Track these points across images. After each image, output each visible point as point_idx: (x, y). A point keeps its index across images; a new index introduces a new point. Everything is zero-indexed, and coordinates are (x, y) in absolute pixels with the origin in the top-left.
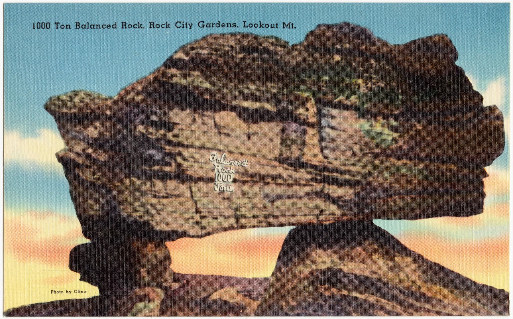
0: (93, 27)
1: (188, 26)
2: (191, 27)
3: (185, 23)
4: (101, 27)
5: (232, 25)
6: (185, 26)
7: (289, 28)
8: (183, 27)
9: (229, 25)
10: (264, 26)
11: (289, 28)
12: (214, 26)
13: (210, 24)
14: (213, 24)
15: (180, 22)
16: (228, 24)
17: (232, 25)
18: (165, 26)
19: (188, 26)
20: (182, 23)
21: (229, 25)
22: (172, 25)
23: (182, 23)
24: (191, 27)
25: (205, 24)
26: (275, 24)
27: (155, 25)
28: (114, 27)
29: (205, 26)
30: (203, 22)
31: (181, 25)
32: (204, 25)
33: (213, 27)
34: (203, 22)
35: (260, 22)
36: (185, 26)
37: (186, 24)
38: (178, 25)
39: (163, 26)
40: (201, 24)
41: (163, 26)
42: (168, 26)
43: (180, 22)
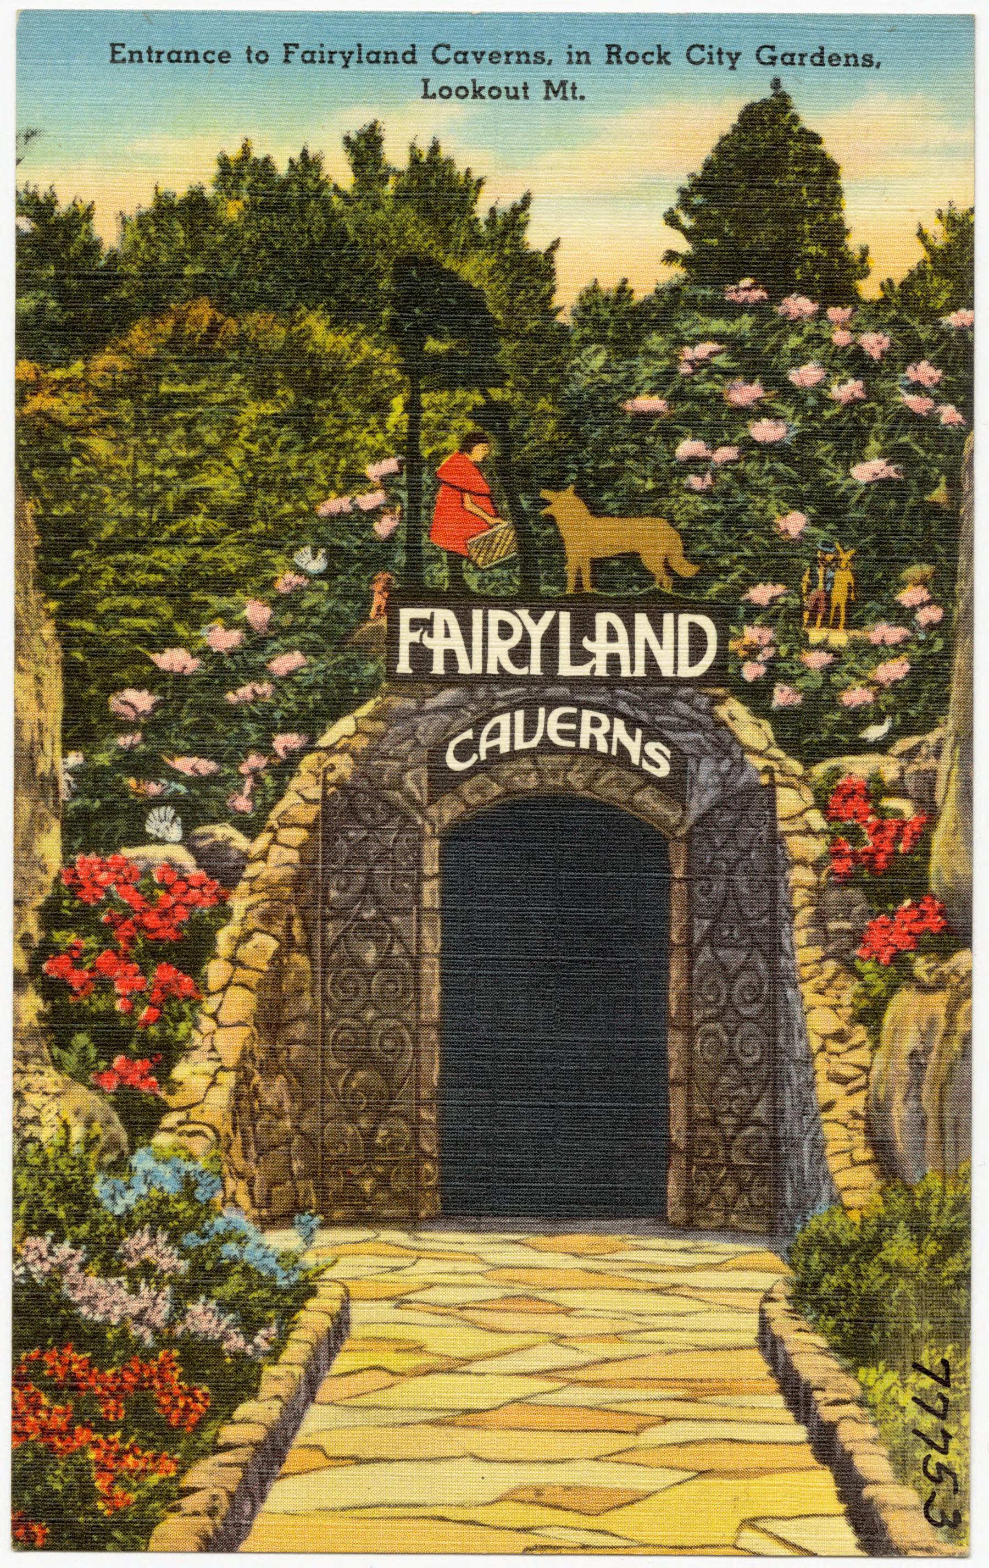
0: (192, 57)
1: (725, 58)
2: (734, 61)
3: (715, 50)
4: (201, 58)
5: (860, 61)
6: (716, 60)
7: (565, 98)
8: (711, 63)
9: (852, 61)
10: (485, 93)
11: (565, 98)
12: (807, 60)
15: (702, 47)
16: (847, 57)
17: (860, 61)
18: (655, 58)
19: (725, 58)
20: (707, 50)
21: (852, 61)
22: (679, 59)
23: (707, 50)
24: (734, 61)
25: (778, 53)
26: (520, 86)
28: (409, 57)
29: (779, 61)
30: (772, 48)
31: (704, 54)
32: (774, 58)
33: (802, 64)
34: (772, 48)
35: (474, 81)
36: (716, 60)
38: (696, 54)
39: (648, 58)
40: (765, 54)
41: (648, 58)
42: (663, 58)
43: (702, 47)
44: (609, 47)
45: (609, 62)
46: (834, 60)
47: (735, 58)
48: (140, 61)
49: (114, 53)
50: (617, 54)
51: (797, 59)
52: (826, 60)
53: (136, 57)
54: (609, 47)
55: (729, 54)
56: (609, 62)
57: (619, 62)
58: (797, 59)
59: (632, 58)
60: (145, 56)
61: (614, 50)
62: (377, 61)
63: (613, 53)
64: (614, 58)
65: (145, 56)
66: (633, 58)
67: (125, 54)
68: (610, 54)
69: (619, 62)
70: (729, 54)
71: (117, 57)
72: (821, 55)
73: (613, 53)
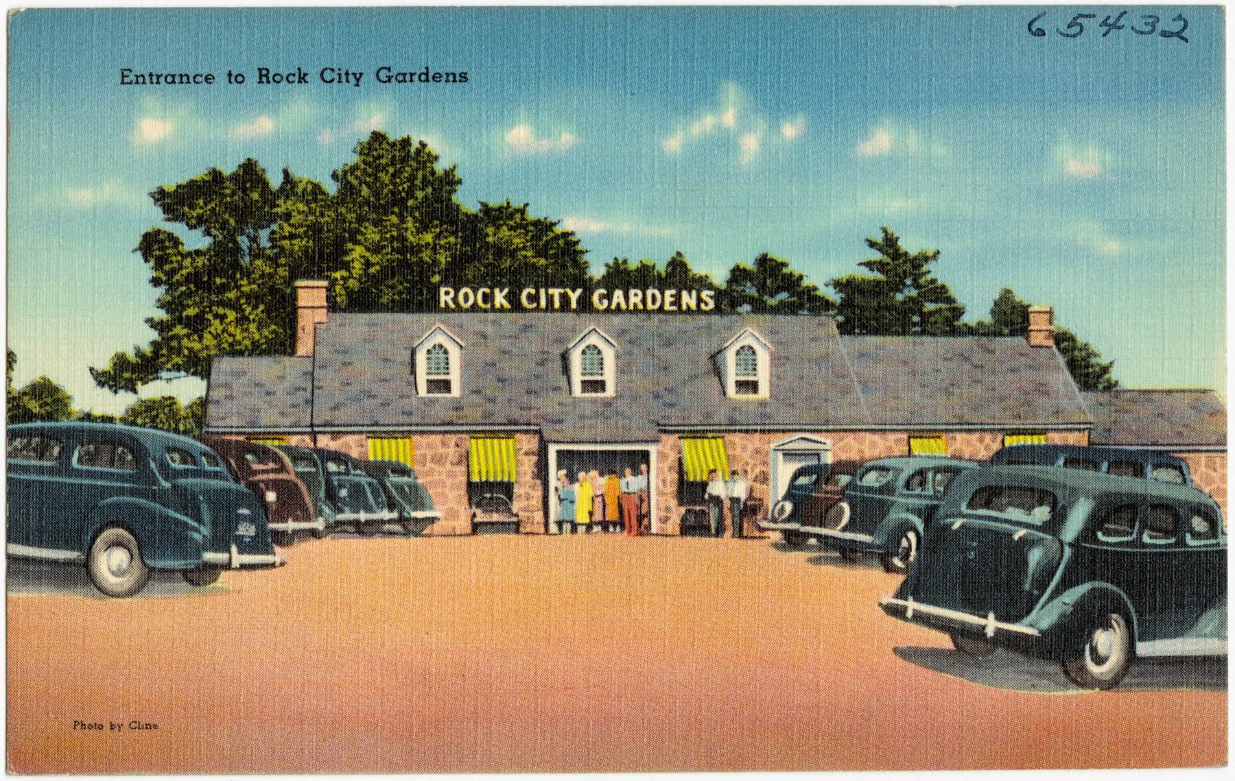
1: (351, 78)
6: (344, 77)
9: (451, 78)
12: (416, 78)
13: (405, 75)
14: (412, 75)
15: (333, 70)
16: (448, 75)
17: (458, 78)
18: (297, 79)
19: (351, 78)
20: (337, 71)
22: (313, 76)
23: (337, 71)
24: (358, 80)
25: (393, 72)
27: (271, 76)
33: (411, 81)
36: (344, 77)
37: (347, 74)
40: (383, 75)
42: (302, 79)
43: (333, 70)
44: (260, 70)
45: (261, 82)
46: (437, 77)
47: (358, 78)
48: (144, 83)
49: (124, 76)
50: (266, 76)
51: (408, 78)
52: (430, 78)
53: (141, 80)
54: (260, 70)
55: (354, 74)
56: (261, 82)
57: (268, 82)
58: (408, 78)
59: (277, 78)
60: (147, 80)
61: (264, 72)
62: (173, 82)
63: (264, 75)
64: (264, 79)
65: (147, 80)
66: (277, 79)
67: (132, 78)
68: (261, 76)
69: (268, 82)
70: (354, 74)
71: (126, 80)
72: (427, 74)
73: (264, 75)
